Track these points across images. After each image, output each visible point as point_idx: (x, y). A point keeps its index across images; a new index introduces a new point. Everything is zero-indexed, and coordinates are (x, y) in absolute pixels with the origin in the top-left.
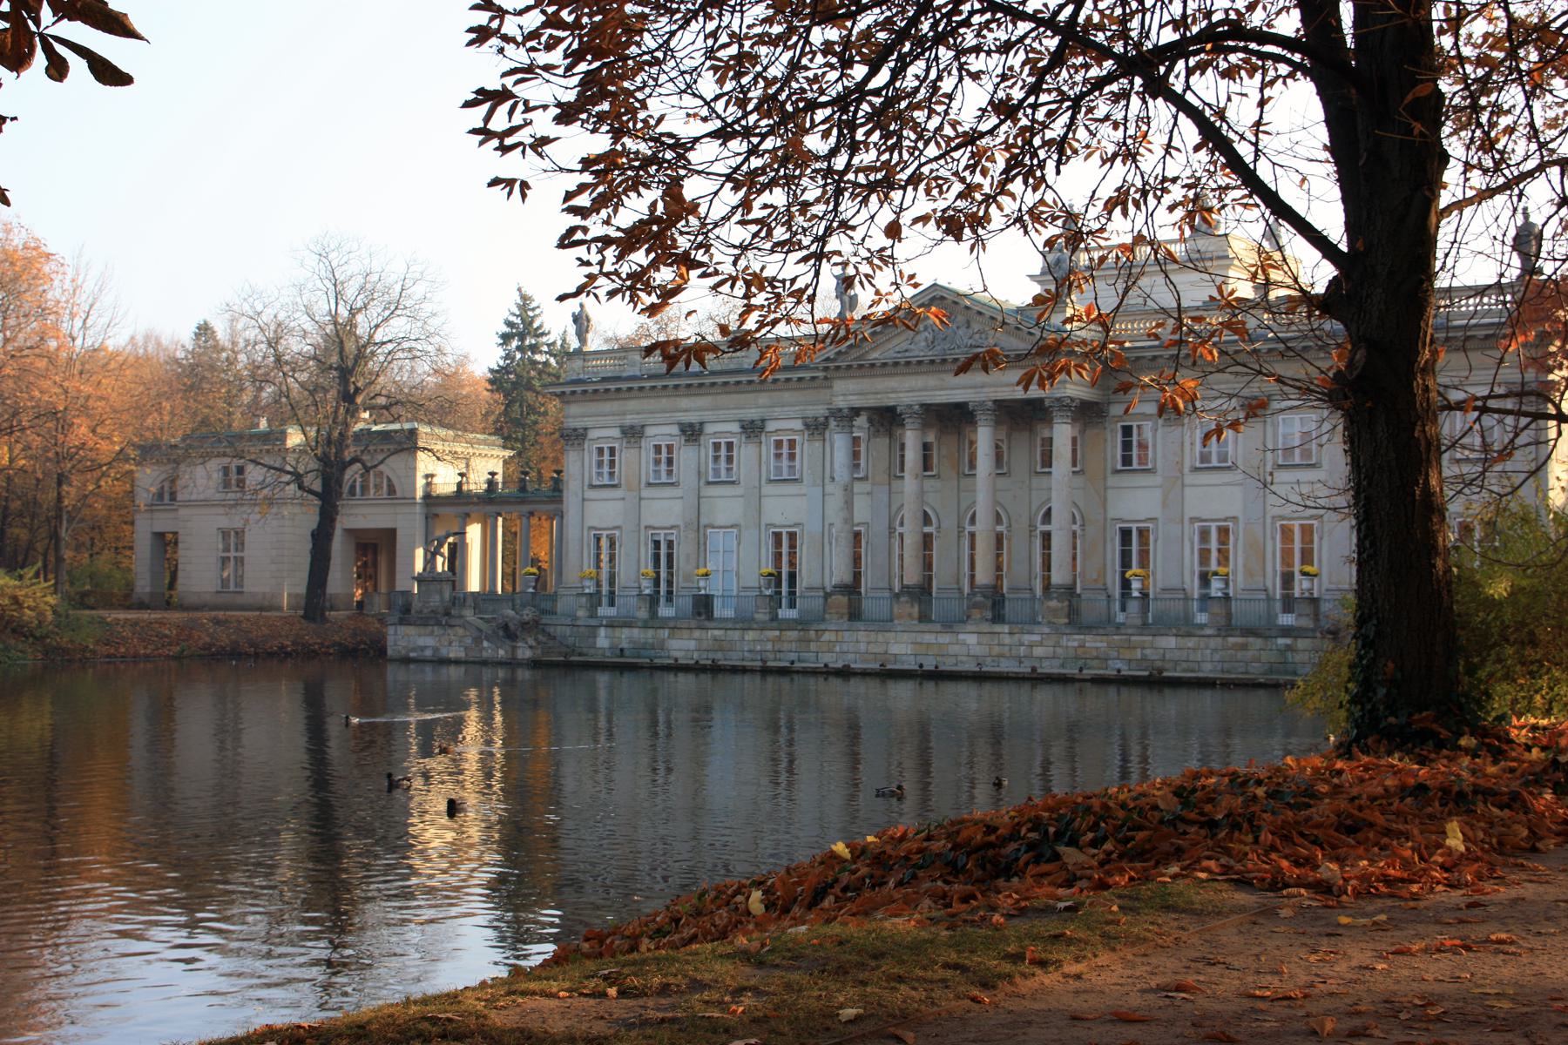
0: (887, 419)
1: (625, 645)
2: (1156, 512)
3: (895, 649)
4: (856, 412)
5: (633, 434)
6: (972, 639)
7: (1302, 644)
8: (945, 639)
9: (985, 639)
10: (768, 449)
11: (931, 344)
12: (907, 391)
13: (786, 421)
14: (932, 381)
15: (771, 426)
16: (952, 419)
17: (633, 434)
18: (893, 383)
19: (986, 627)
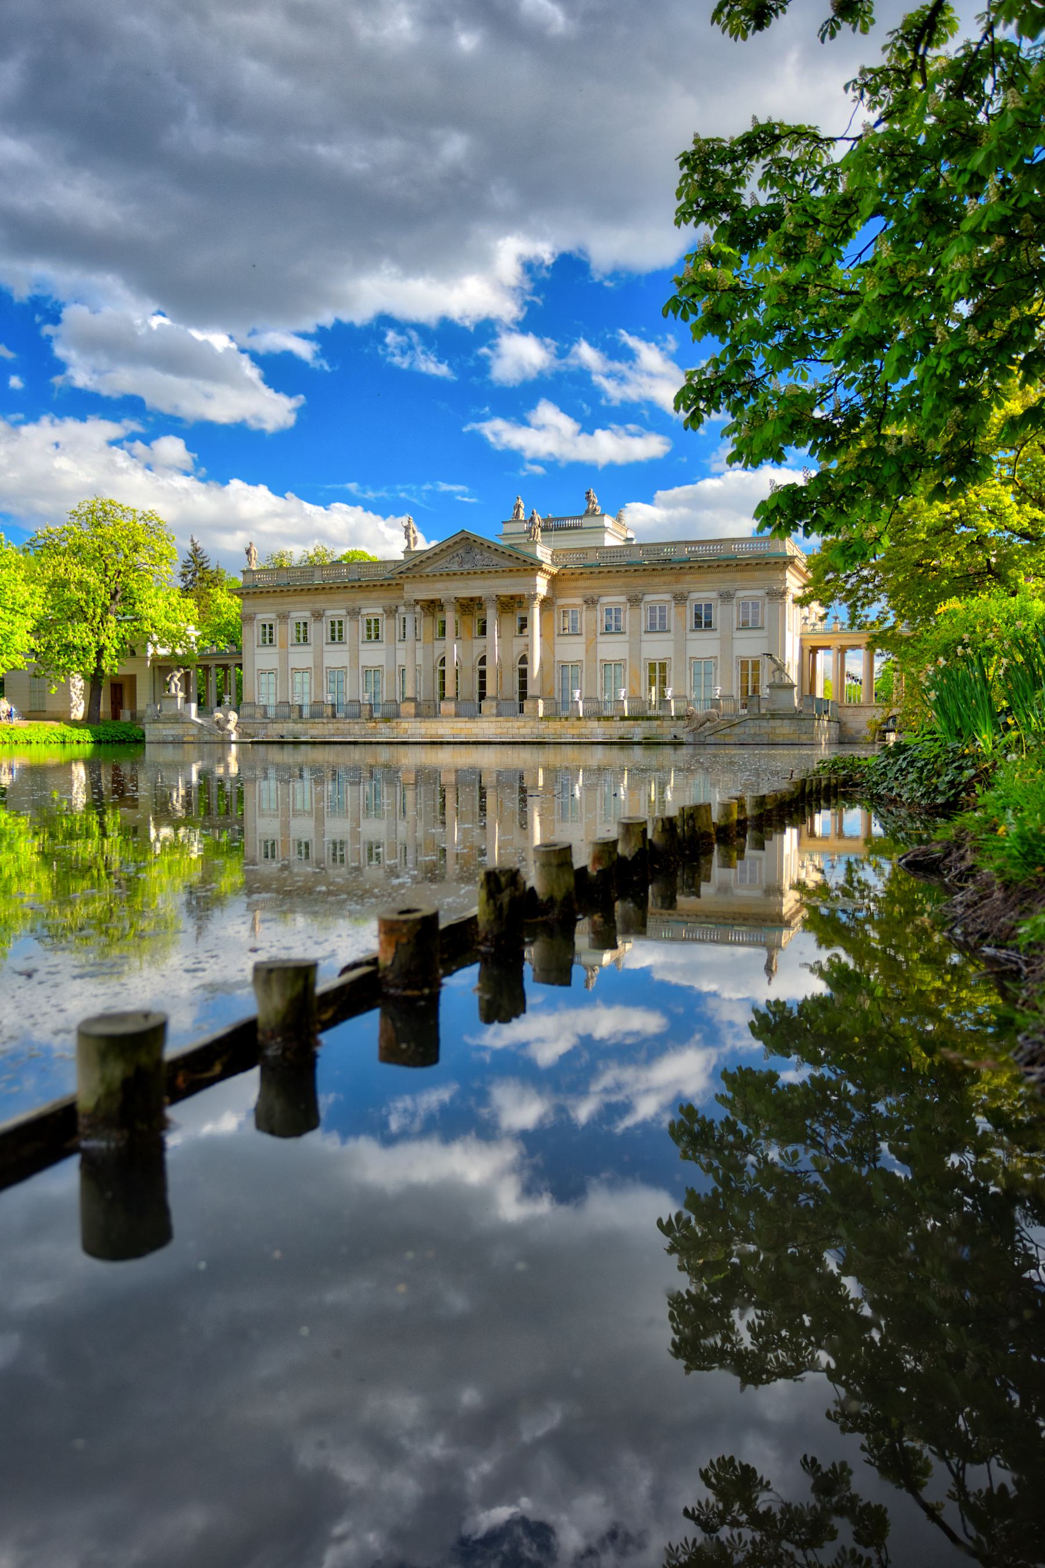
0: (433, 606)
1: (284, 733)
2: (583, 658)
3: (441, 731)
4: (417, 602)
5: (283, 617)
6: (485, 725)
7: (666, 724)
8: (470, 725)
9: (493, 725)
10: (362, 626)
11: (461, 564)
13: (373, 609)
14: (461, 584)
15: (364, 611)
16: (470, 606)
18: (439, 585)
19: (494, 719)
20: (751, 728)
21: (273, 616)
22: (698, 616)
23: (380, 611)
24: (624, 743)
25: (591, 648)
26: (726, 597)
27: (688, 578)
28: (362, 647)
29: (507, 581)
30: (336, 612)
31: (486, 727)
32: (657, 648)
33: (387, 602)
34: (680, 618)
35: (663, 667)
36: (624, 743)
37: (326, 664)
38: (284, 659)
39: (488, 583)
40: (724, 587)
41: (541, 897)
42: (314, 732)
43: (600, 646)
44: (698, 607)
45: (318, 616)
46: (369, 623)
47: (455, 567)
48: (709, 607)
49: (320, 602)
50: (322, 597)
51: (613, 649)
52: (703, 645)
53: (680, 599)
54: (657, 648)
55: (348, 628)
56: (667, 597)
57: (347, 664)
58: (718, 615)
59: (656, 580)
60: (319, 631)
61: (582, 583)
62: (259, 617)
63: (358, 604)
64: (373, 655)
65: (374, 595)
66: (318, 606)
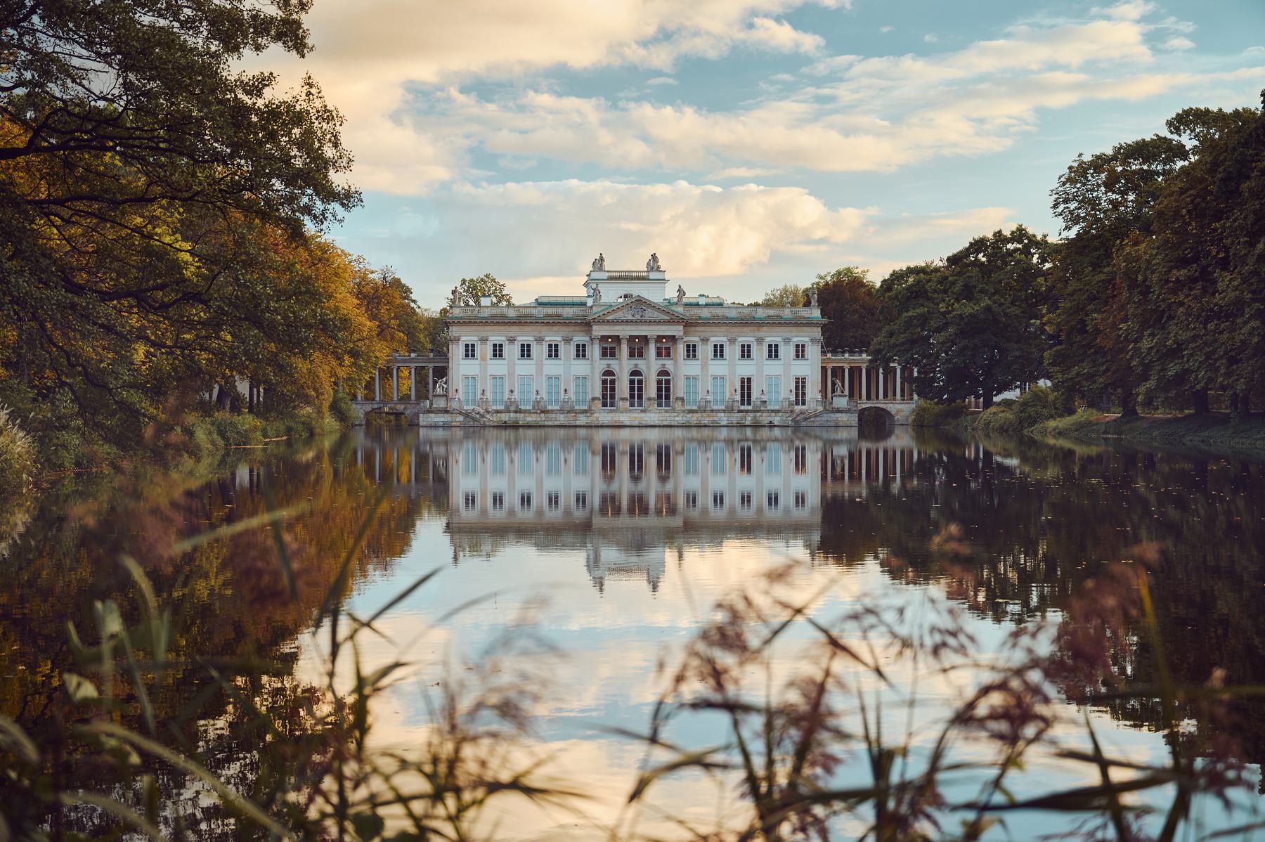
12: (625, 331)
13: (554, 337)
14: (633, 328)
15: (547, 339)
17: (484, 340)
20: (826, 417)
21: (475, 338)
22: (770, 351)
23: (559, 339)
24: (687, 426)
25: (704, 366)
26: (787, 341)
27: (765, 329)
28: (546, 362)
29: (664, 328)
30: (525, 337)
31: (653, 417)
32: (746, 369)
33: (565, 334)
34: (759, 352)
35: (749, 380)
36: (687, 426)
37: (517, 372)
38: (483, 369)
39: (651, 328)
40: (786, 335)
41: (114, 606)
42: (529, 419)
43: (710, 367)
44: (770, 346)
45: (512, 340)
46: (550, 346)
47: (630, 317)
48: (776, 346)
49: (513, 331)
50: (515, 328)
51: (718, 368)
52: (773, 368)
53: (760, 341)
54: (746, 369)
55: (535, 349)
56: (752, 339)
57: (533, 372)
58: (782, 350)
59: (745, 329)
60: (512, 351)
61: (699, 329)
62: (463, 338)
63: (543, 334)
64: (552, 367)
65: (555, 328)
66: (511, 334)
